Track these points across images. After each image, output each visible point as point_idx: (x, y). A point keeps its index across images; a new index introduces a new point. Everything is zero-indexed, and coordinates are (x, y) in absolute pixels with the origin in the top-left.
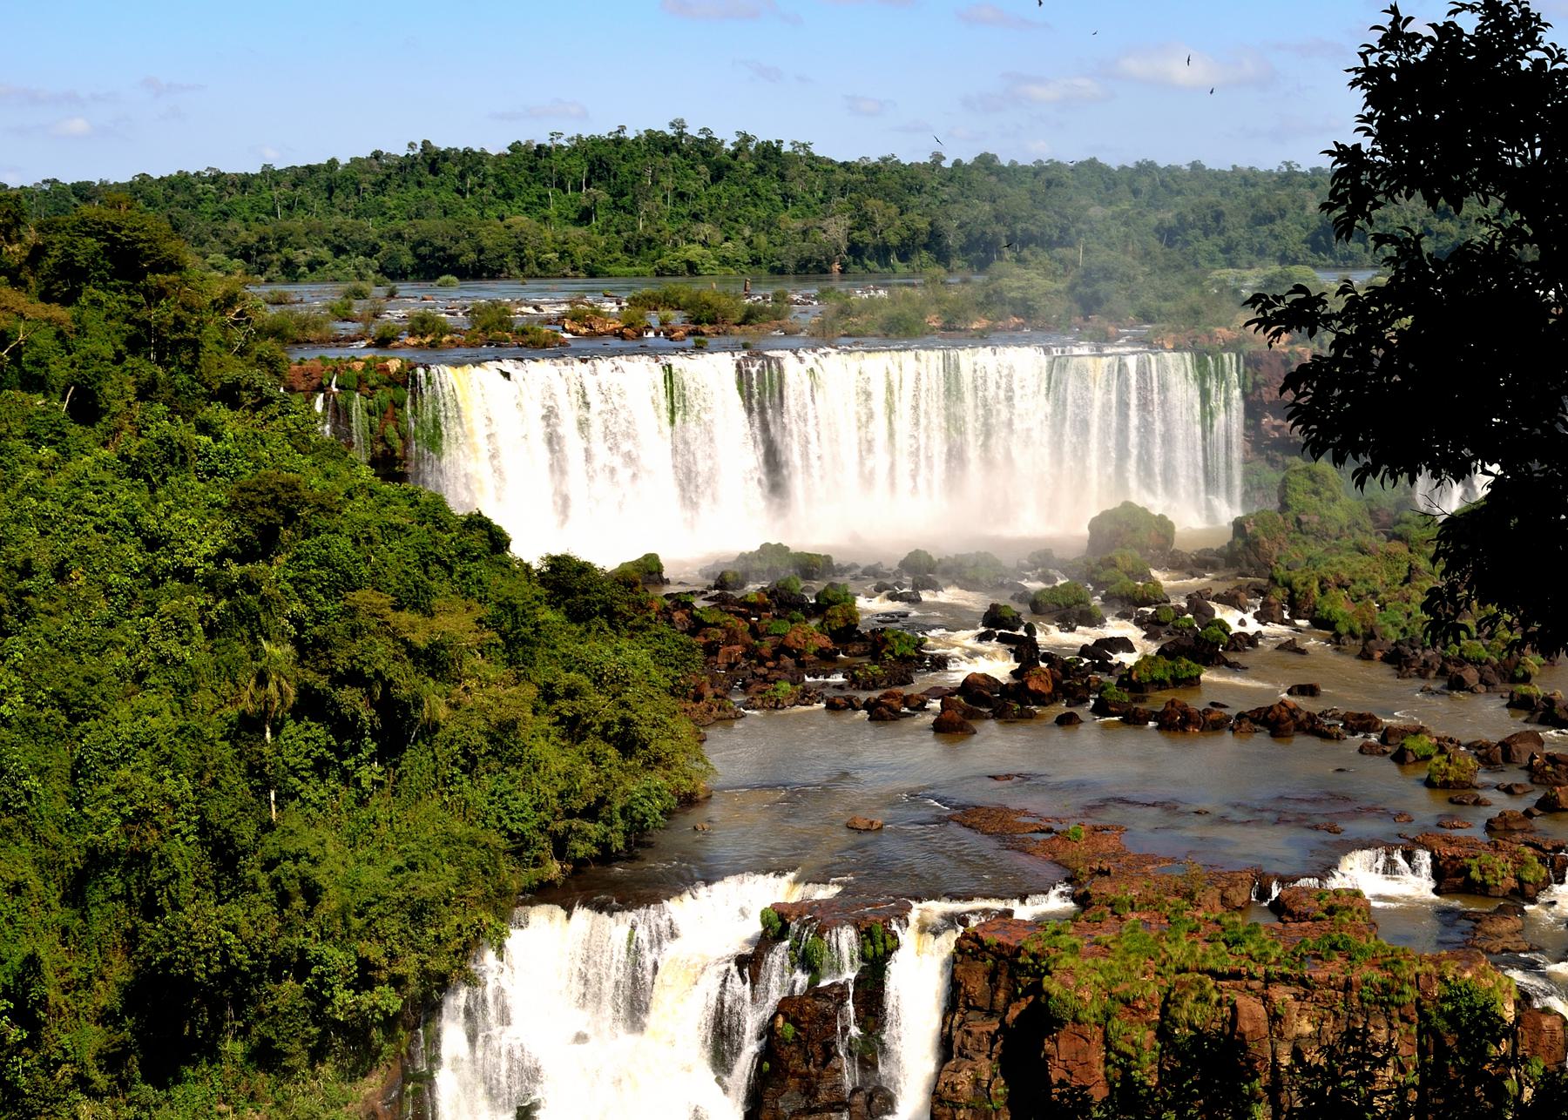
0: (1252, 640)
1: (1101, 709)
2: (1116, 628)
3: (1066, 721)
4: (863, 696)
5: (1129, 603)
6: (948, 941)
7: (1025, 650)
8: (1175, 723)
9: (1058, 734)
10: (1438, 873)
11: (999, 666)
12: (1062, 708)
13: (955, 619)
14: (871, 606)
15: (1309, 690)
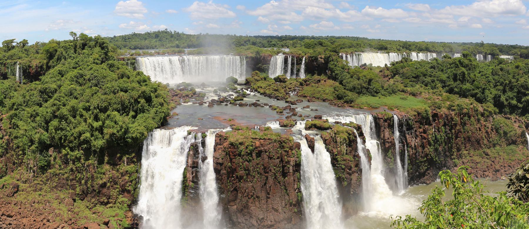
0: (250, 94)
1: (230, 103)
2: (231, 93)
3: (227, 105)
4: (198, 102)
5: (234, 90)
6: (214, 135)
7: (219, 96)
8: (241, 105)
9: (225, 107)
10: (279, 124)
11: (216, 98)
12: (225, 103)
13: (210, 92)
14: (198, 90)
15: (259, 101)
